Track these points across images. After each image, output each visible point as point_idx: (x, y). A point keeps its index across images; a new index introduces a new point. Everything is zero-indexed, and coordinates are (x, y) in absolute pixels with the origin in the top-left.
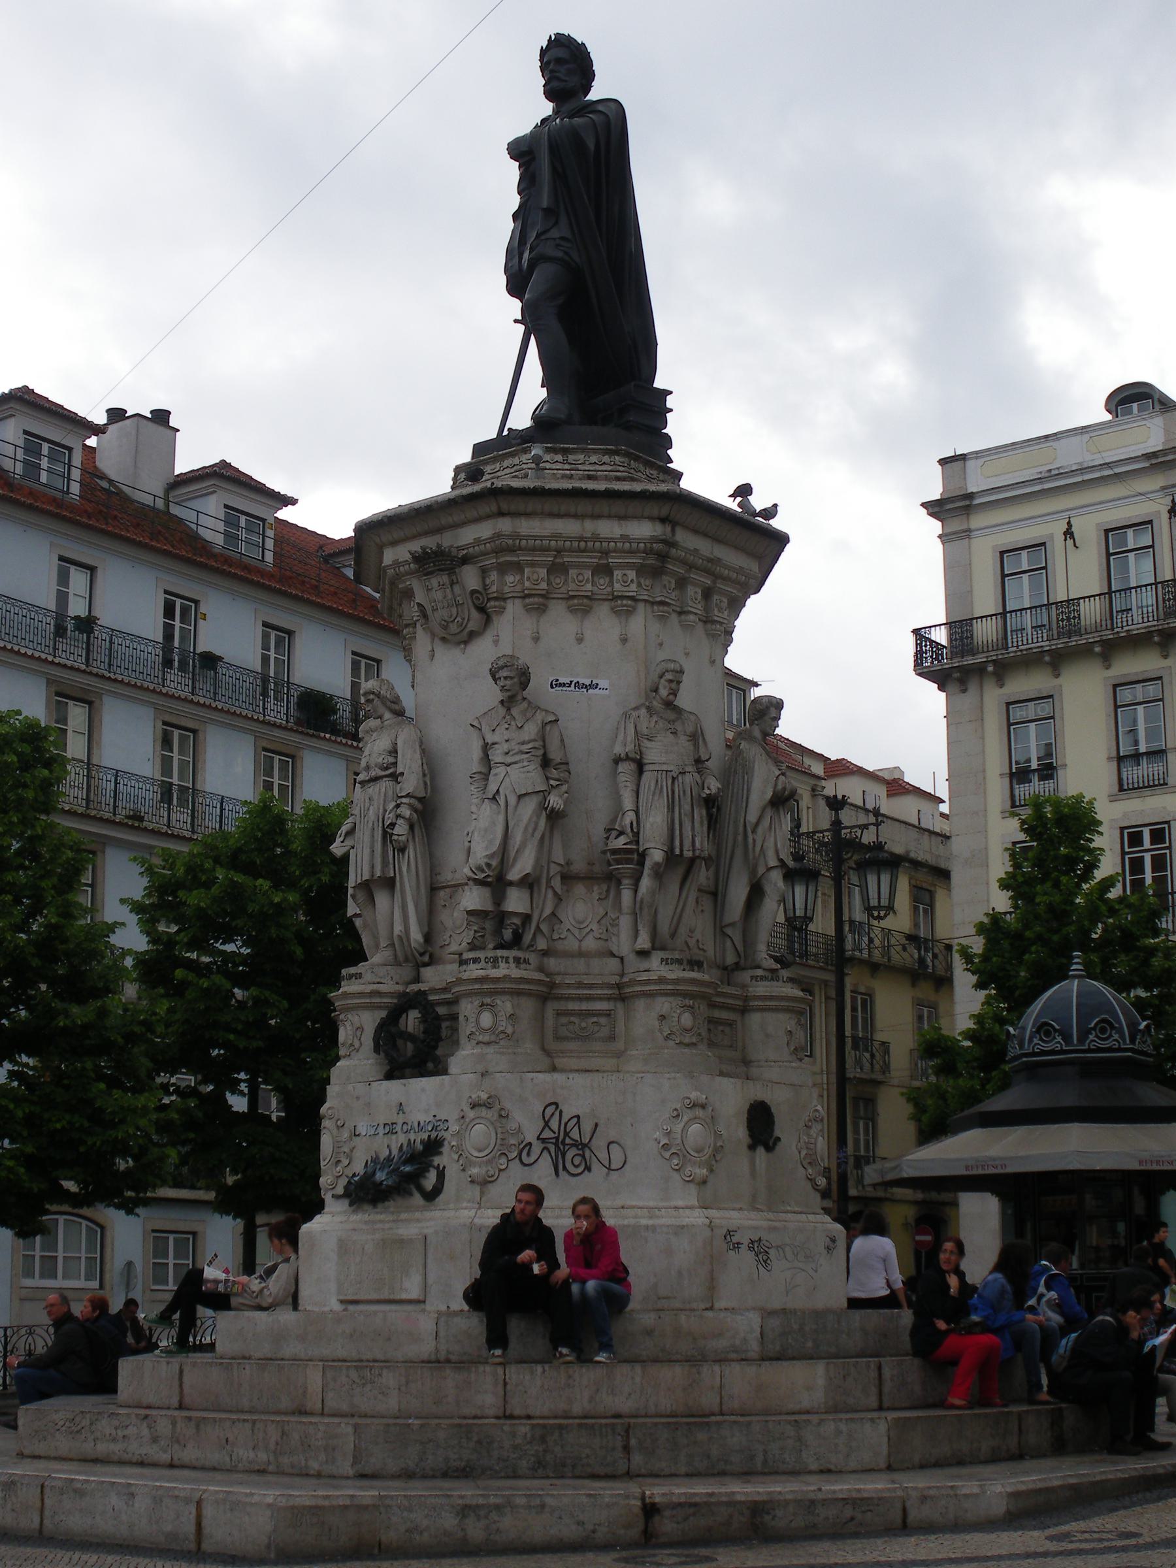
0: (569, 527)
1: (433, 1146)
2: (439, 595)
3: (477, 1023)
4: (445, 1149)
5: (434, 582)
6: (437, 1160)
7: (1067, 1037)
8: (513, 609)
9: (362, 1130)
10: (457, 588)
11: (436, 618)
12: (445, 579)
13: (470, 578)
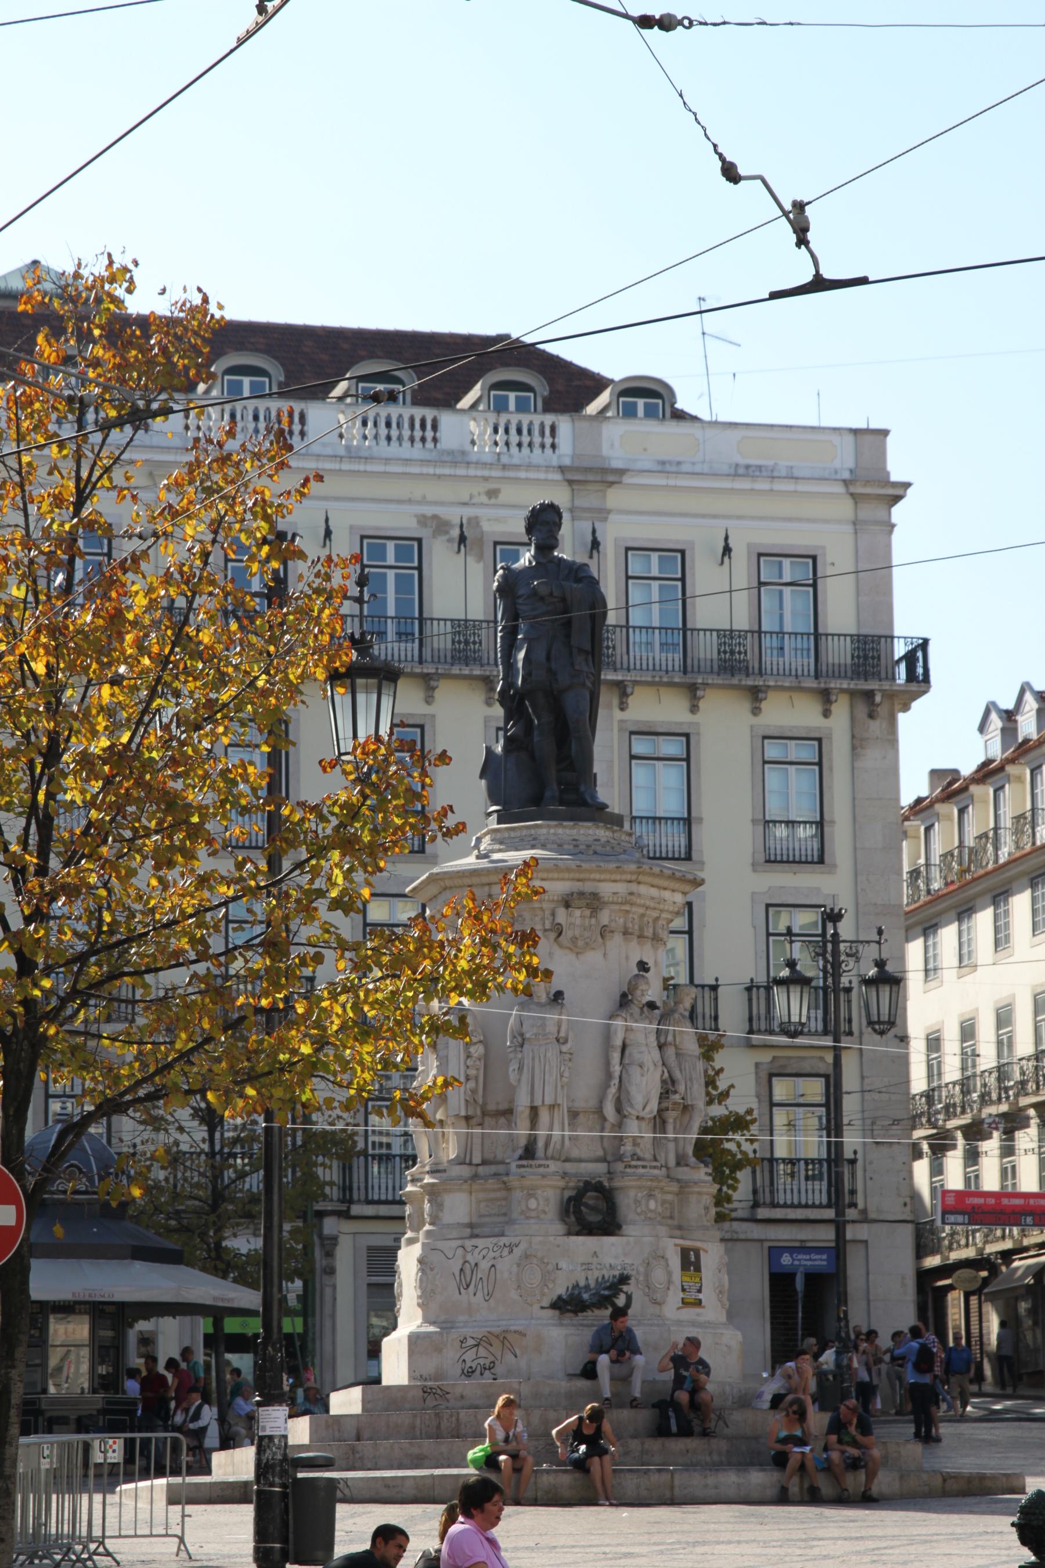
0: (654, 892)
1: (624, 1279)
2: (578, 922)
3: (647, 1206)
4: (632, 1281)
5: (577, 913)
6: (625, 1288)
7: (91, 1180)
8: (618, 938)
9: (563, 1265)
10: (593, 921)
11: (568, 933)
12: (588, 912)
13: (605, 917)
